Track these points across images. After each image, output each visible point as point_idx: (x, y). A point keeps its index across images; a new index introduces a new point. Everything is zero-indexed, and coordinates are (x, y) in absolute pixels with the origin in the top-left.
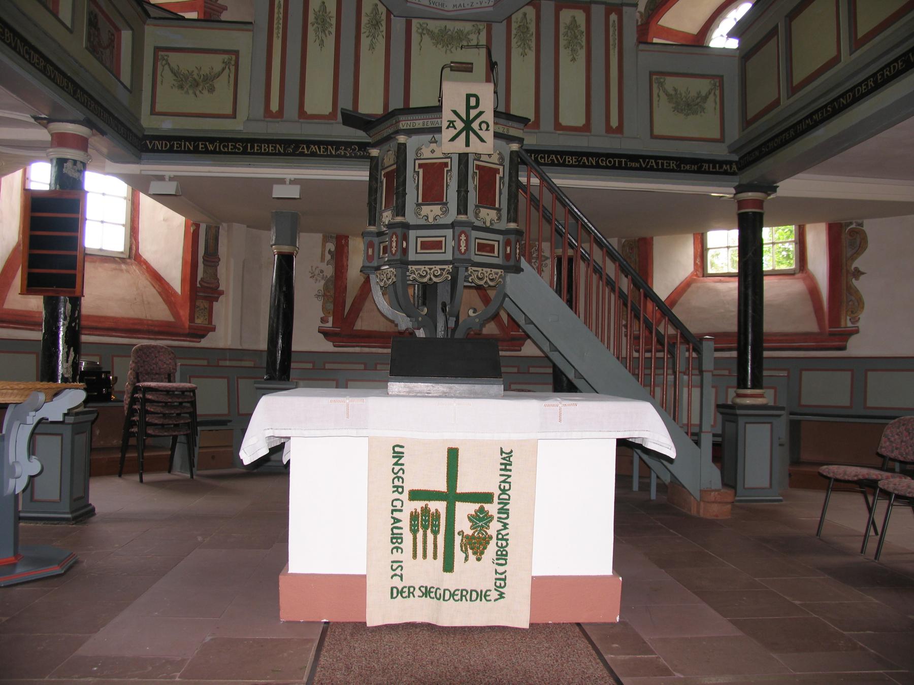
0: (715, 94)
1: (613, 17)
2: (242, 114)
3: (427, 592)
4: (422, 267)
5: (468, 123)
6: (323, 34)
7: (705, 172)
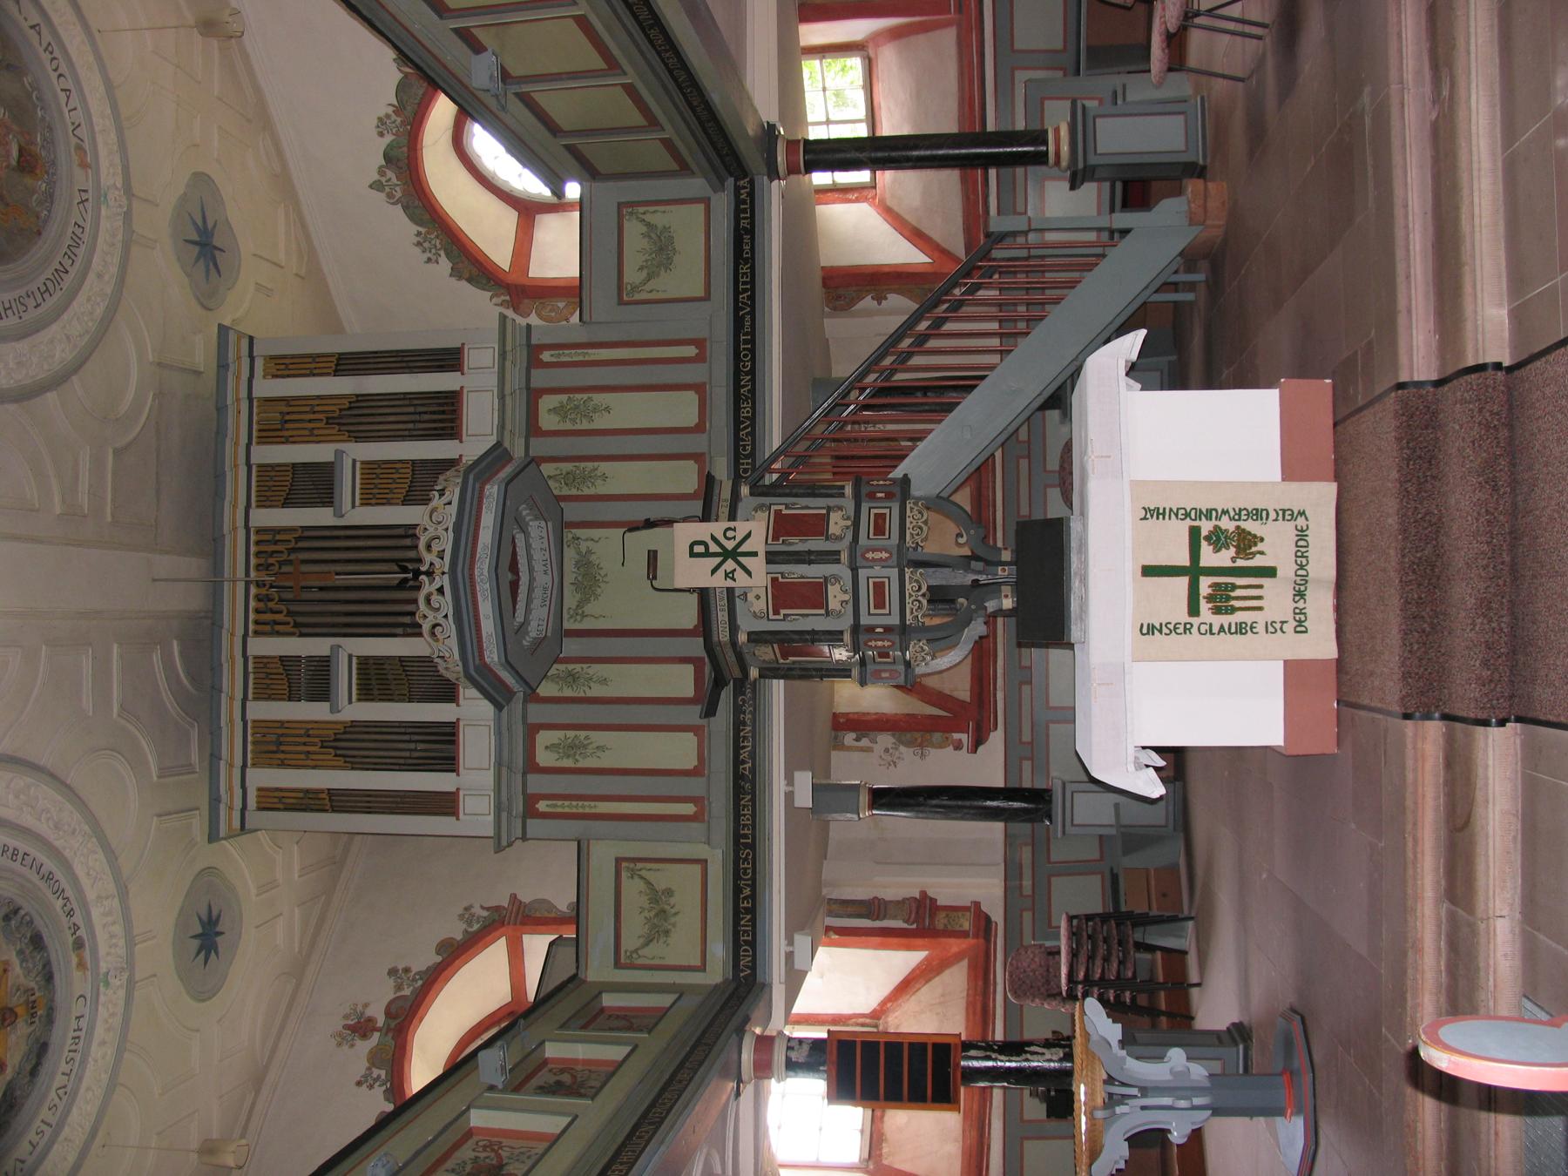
0: (644, 213)
1: (546, 356)
2: (701, 851)
3: (1300, 595)
4: (908, 607)
5: (727, 554)
6: (590, 747)
7: (752, 223)
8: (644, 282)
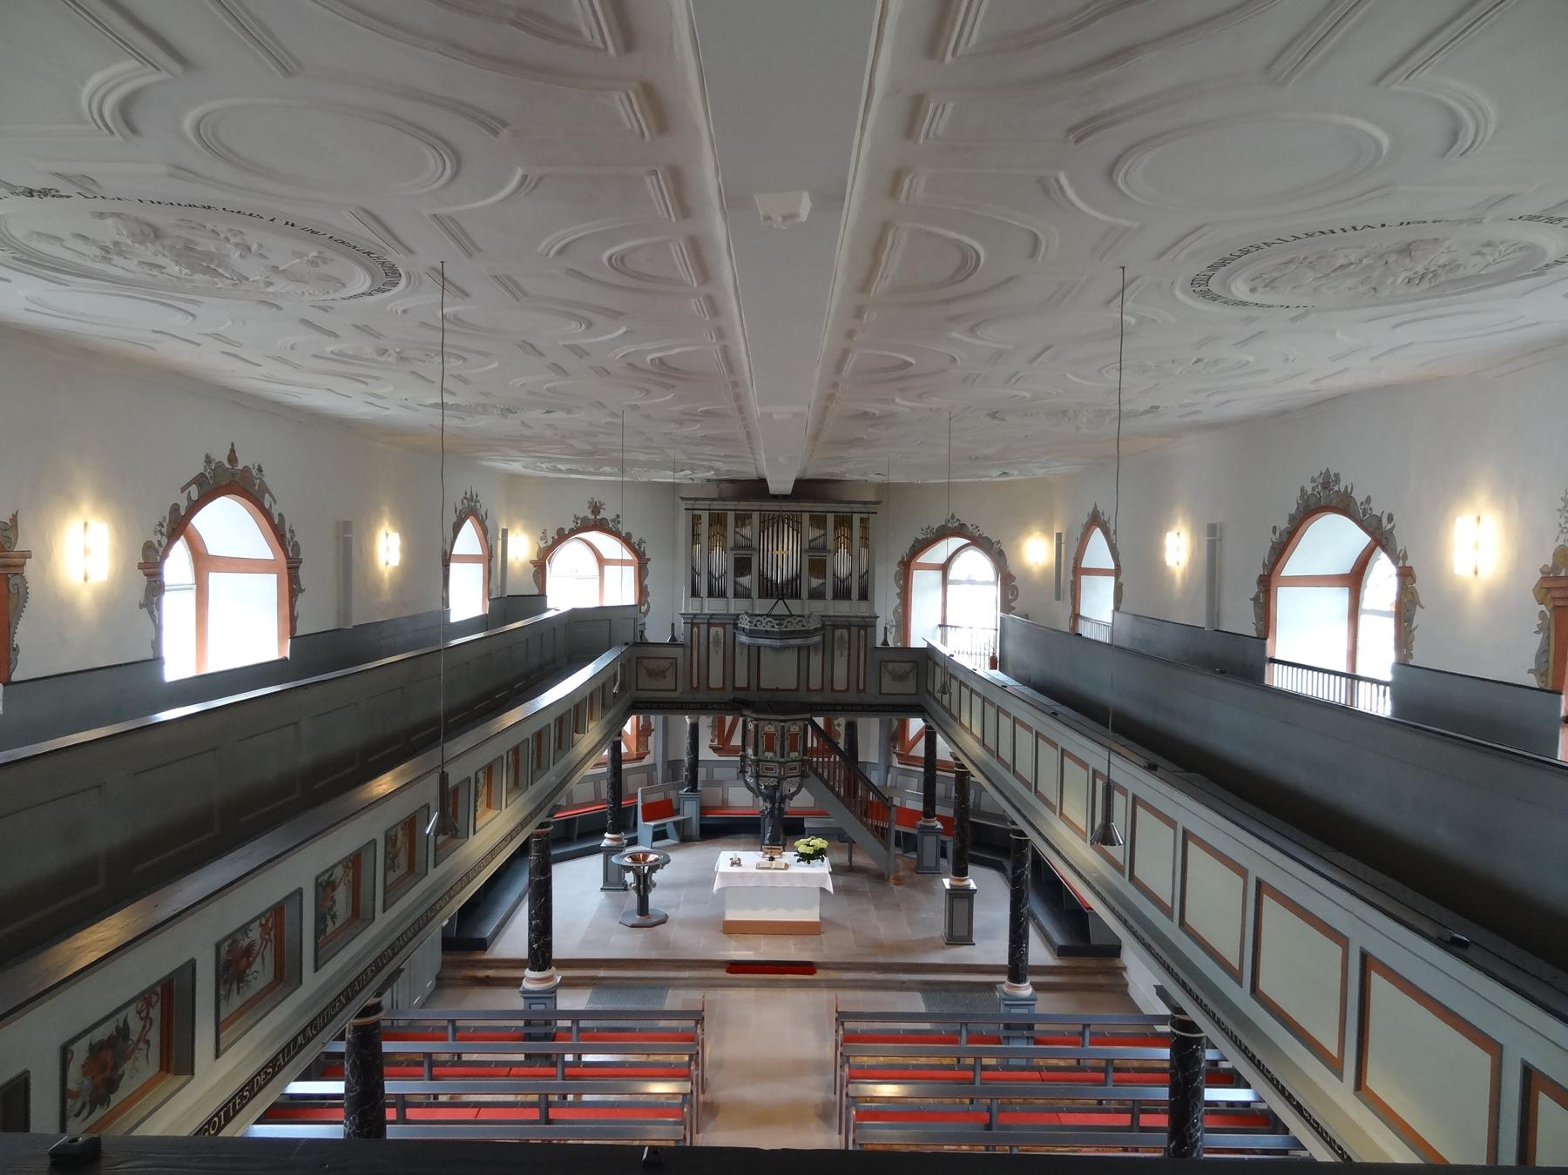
1: (862, 632)
2: (680, 689)
8: (888, 671)
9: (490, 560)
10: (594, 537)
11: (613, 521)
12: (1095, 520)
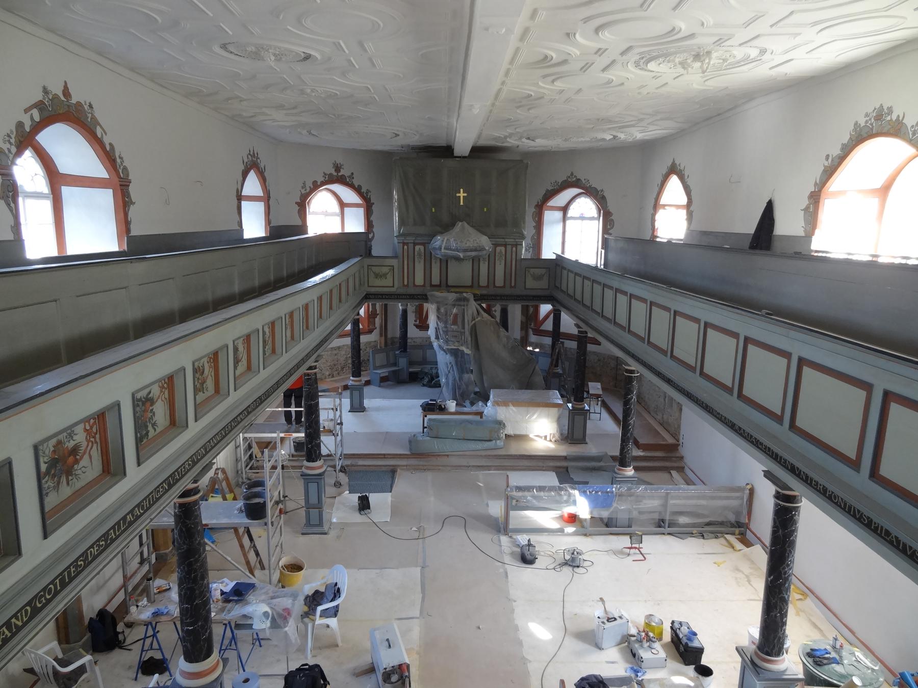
1: (514, 249)
9: (268, 200)
10: (337, 188)
11: (349, 177)
12: (674, 170)
